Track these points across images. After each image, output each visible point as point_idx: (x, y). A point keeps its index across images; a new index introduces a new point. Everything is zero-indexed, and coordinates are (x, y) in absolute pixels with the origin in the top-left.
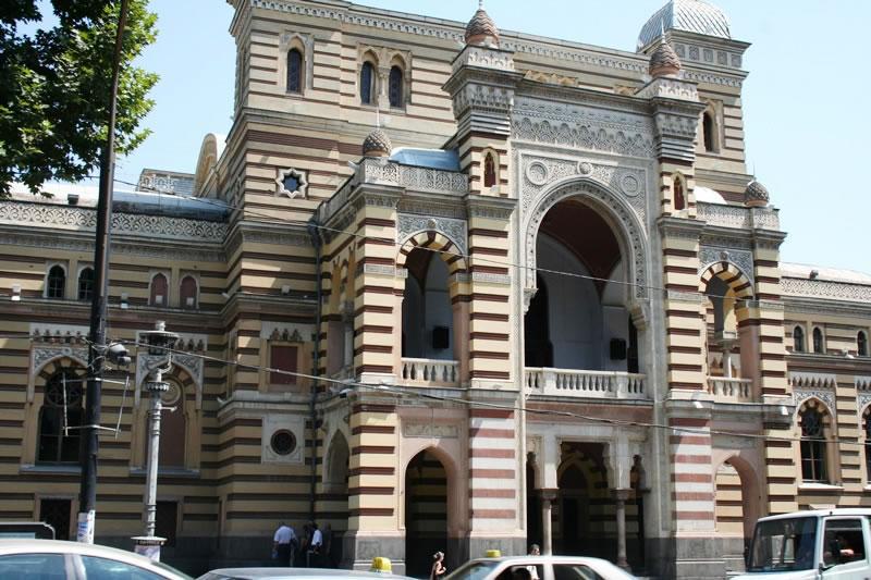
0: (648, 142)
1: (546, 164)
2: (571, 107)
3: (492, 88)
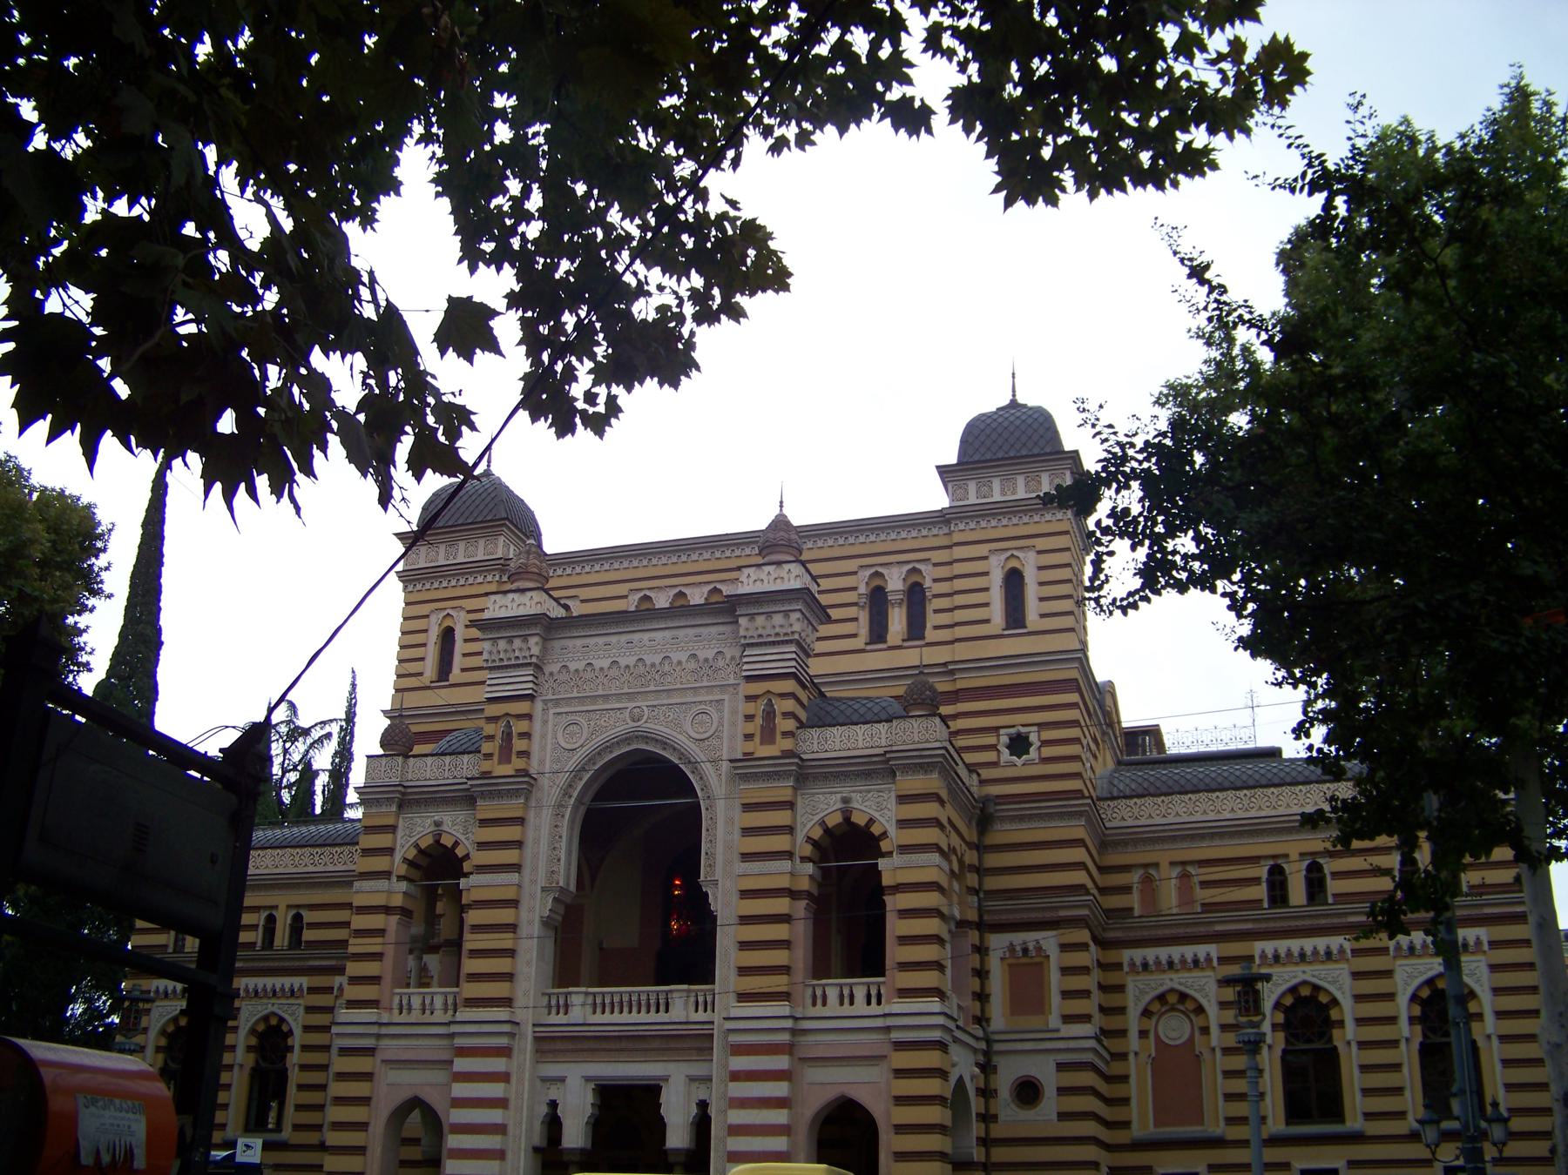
0: (733, 658)
1: (582, 720)
2: (624, 638)
3: (510, 640)
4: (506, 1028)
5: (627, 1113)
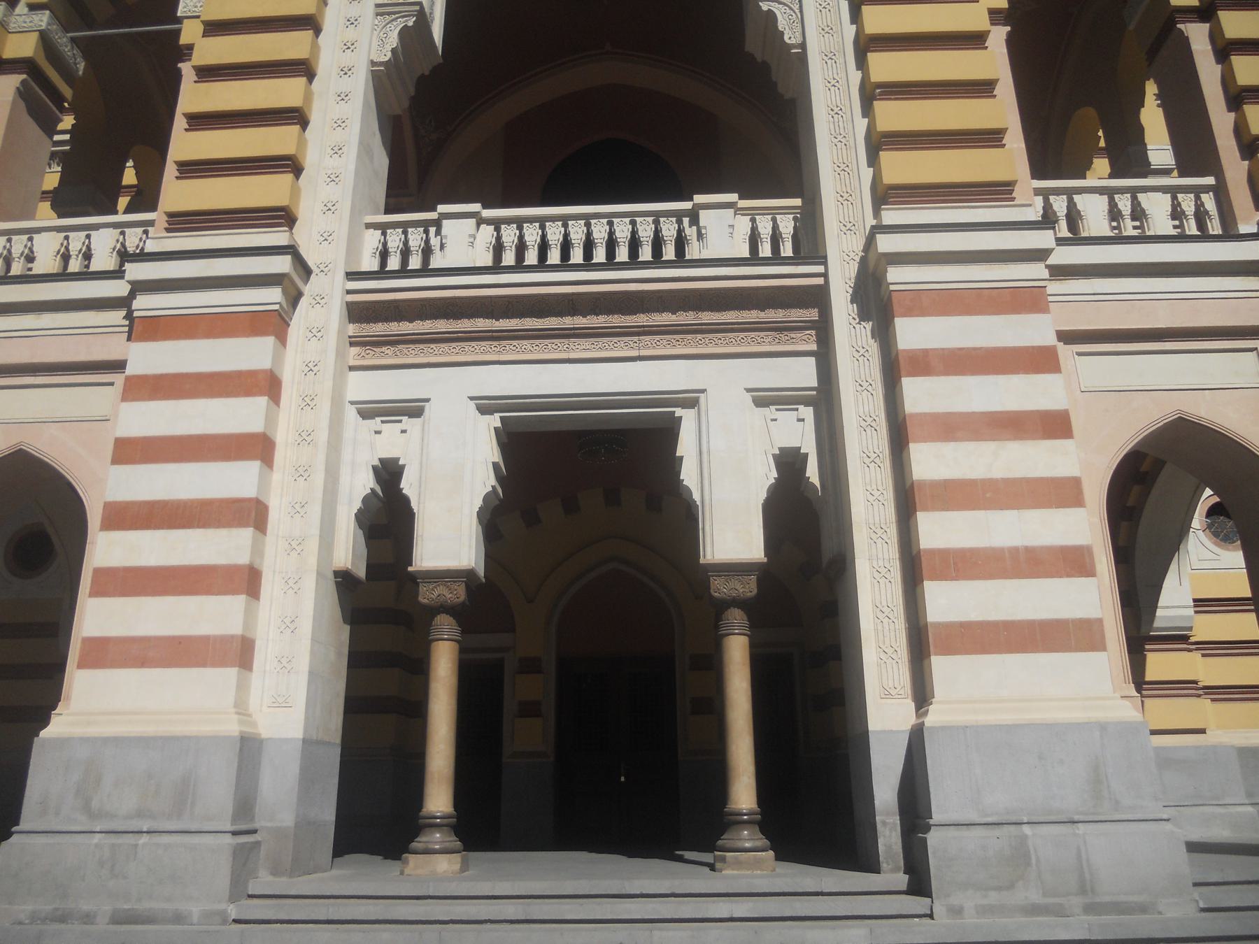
4: (282, 264)
5: (587, 482)
